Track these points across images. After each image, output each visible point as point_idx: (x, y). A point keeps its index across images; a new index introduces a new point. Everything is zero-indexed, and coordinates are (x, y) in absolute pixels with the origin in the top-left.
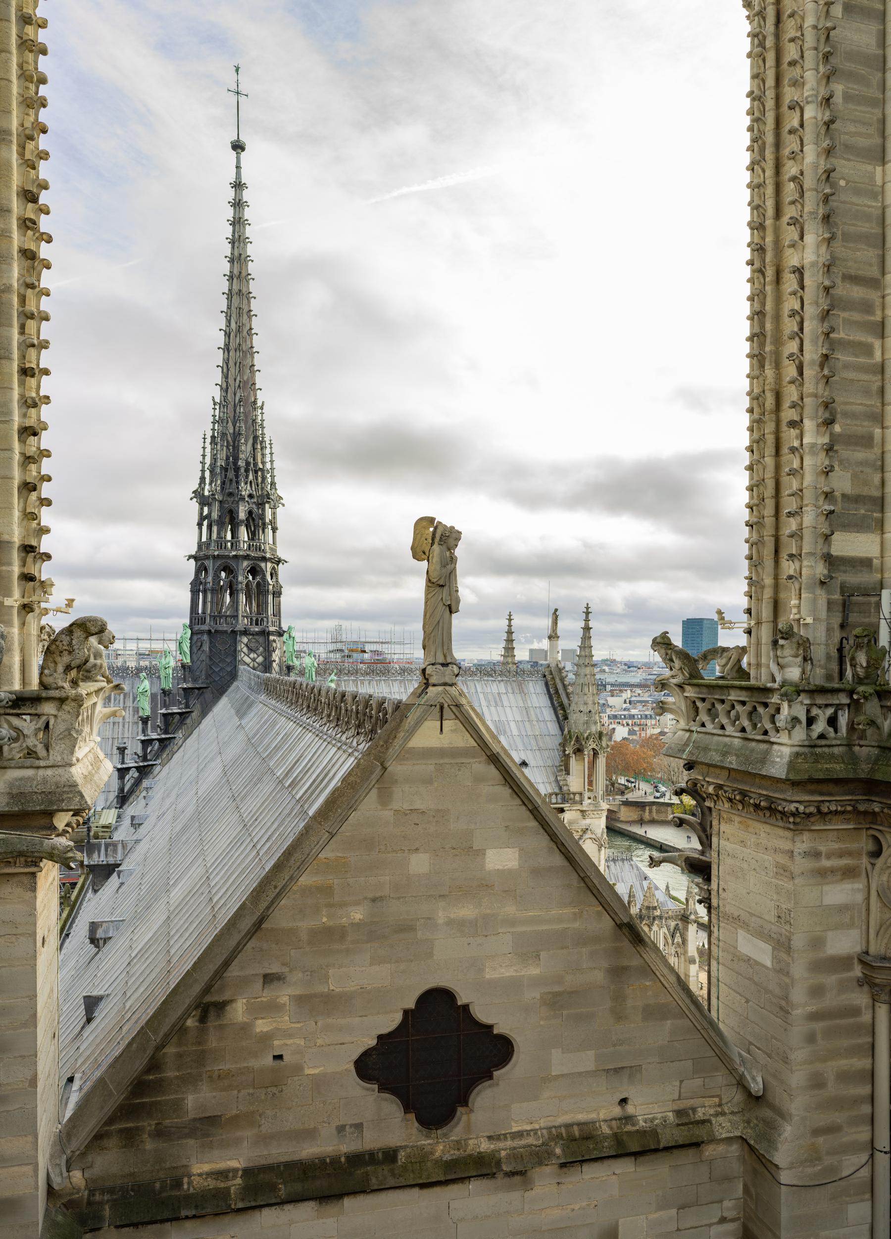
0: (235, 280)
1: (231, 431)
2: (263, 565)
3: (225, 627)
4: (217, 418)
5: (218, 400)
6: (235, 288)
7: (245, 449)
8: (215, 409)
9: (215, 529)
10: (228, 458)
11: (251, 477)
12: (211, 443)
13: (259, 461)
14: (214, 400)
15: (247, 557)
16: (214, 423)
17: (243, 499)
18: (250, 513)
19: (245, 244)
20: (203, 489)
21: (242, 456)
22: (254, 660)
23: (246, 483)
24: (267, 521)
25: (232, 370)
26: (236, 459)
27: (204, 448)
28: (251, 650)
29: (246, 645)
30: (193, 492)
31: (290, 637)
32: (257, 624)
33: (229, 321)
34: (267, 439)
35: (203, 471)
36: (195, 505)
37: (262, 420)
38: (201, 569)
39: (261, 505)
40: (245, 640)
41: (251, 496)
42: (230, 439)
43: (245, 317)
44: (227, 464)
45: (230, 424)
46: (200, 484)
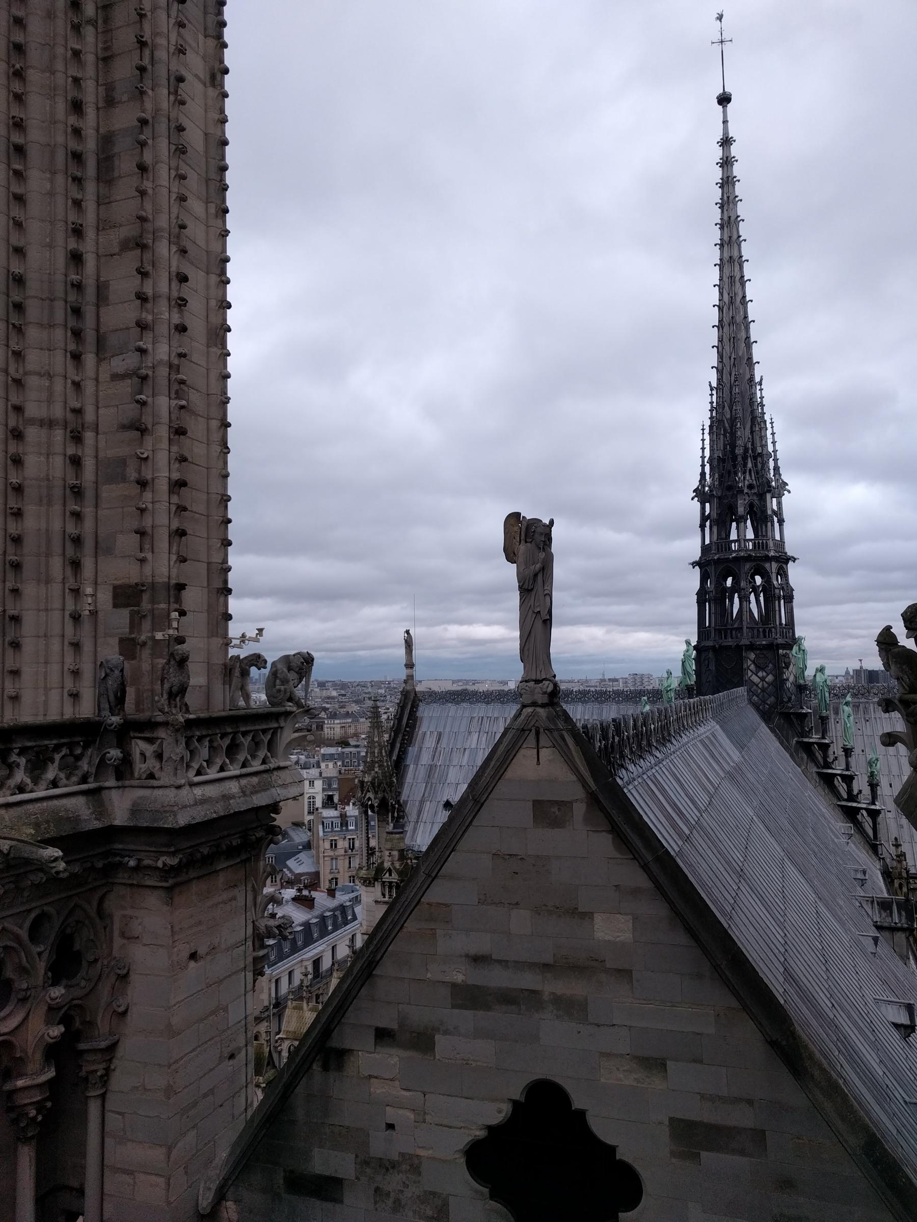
0: (726, 246)
1: (728, 416)
2: (767, 565)
3: (730, 642)
4: (715, 404)
5: (714, 384)
6: (726, 255)
7: (743, 434)
8: (712, 395)
9: (715, 529)
10: (725, 448)
11: (750, 465)
12: (710, 434)
13: (759, 445)
14: (710, 385)
15: (748, 558)
16: (711, 411)
17: (741, 491)
18: (751, 505)
19: (735, 204)
20: (704, 486)
21: (739, 442)
22: (763, 679)
23: (744, 473)
24: (769, 512)
25: (727, 348)
26: (733, 446)
27: (703, 440)
28: (759, 668)
29: (754, 662)
30: (694, 491)
31: (799, 649)
32: (765, 637)
33: (721, 294)
34: (767, 417)
35: (703, 466)
36: (696, 504)
37: (762, 398)
38: (704, 579)
39: (762, 497)
40: (752, 656)
41: (751, 487)
42: (727, 425)
43: (738, 284)
44: (724, 455)
45: (727, 408)
46: (700, 481)
